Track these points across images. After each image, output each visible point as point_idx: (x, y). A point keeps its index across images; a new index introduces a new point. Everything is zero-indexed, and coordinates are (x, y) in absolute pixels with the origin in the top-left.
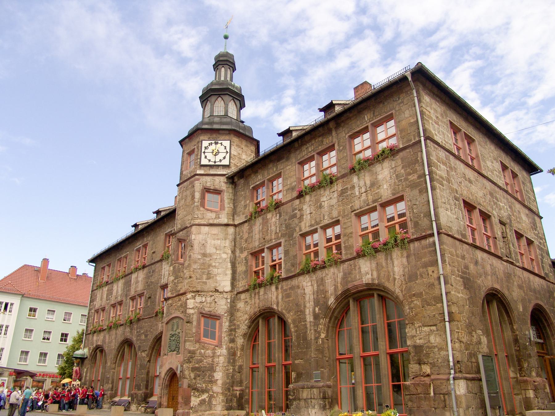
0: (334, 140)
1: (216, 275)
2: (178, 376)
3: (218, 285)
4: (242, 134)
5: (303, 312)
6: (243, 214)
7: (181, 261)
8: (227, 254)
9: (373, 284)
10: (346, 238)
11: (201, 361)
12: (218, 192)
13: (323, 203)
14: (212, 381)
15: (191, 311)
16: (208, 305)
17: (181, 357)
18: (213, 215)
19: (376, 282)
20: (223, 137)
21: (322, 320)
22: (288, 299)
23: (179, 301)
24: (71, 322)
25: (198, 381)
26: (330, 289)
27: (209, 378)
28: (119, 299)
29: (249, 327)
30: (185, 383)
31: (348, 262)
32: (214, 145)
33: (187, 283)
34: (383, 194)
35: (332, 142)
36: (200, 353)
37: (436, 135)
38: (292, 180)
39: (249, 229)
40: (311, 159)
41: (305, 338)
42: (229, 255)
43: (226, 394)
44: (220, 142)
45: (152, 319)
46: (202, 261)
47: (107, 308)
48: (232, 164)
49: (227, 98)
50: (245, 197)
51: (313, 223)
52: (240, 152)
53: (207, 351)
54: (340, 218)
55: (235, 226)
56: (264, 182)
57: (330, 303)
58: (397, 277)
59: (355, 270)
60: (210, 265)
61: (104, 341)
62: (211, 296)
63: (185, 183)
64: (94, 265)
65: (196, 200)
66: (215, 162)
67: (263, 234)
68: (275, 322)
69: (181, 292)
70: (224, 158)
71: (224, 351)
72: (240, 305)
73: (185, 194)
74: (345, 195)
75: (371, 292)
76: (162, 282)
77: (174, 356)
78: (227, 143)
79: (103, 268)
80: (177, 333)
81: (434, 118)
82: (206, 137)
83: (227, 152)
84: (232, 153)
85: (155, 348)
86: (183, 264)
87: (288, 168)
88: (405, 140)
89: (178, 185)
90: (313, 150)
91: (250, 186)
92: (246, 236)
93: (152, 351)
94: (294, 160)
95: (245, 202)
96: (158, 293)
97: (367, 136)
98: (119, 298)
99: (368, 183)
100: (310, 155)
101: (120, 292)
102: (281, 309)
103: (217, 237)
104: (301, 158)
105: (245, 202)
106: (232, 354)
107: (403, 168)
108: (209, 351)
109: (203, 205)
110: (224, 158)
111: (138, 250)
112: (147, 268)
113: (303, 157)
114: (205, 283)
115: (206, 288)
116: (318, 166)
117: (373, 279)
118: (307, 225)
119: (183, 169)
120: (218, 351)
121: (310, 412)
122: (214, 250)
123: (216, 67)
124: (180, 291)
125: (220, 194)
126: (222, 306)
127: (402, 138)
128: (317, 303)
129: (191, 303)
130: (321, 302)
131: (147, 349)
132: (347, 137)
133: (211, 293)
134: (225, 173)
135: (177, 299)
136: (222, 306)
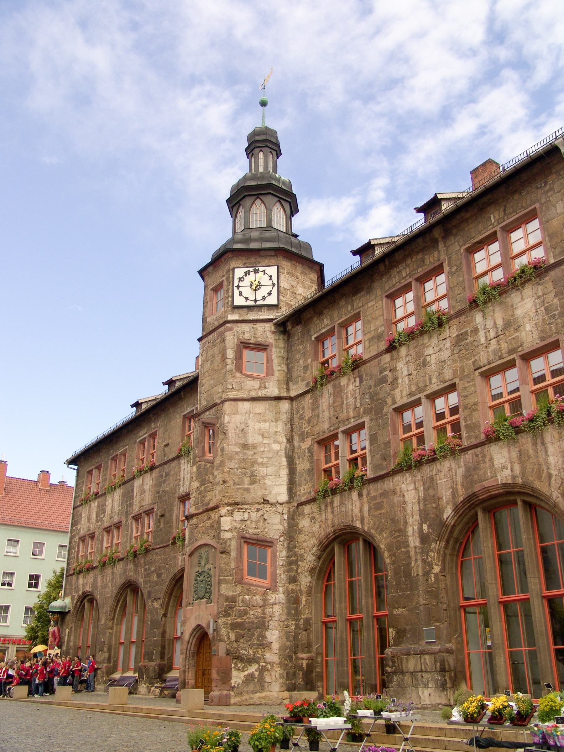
0: (442, 257)
1: (264, 478)
2: (211, 637)
3: (267, 492)
4: (295, 254)
5: (402, 532)
6: (303, 380)
7: (209, 456)
8: (280, 444)
9: (514, 485)
10: (467, 412)
11: (245, 613)
12: (261, 347)
13: (428, 358)
14: (264, 645)
15: (228, 535)
16: (254, 524)
17: (214, 607)
18: (256, 384)
19: (520, 481)
20: (266, 262)
21: (433, 545)
22: (379, 512)
23: (208, 519)
24: (43, 557)
25: (242, 645)
26: (446, 494)
27: (258, 640)
28: (116, 519)
29: (319, 558)
30: (221, 648)
31: (473, 451)
32: (252, 274)
33: (220, 492)
34: (524, 340)
35: (439, 260)
36: (244, 601)
38: (378, 323)
39: (313, 403)
40: (407, 288)
41: (408, 574)
42: (283, 446)
43: (287, 665)
44: (261, 269)
45: (167, 549)
46: (241, 456)
47: (97, 533)
48: (281, 303)
49: (269, 199)
50: (304, 354)
51: (414, 389)
52: (294, 283)
53: (254, 598)
54: (457, 381)
55: (291, 399)
56: (333, 328)
57: (445, 516)
58: (554, 472)
59: (484, 462)
60: (254, 463)
61: (94, 585)
62: (258, 510)
63: (211, 336)
64: (76, 467)
65: (229, 361)
66: (256, 301)
67: (335, 411)
68: (359, 548)
69: (211, 505)
70: (270, 294)
71: (281, 597)
72: (304, 523)
73: (210, 353)
74: (463, 343)
75: (512, 498)
76: (181, 491)
77: (203, 606)
78: (272, 271)
79: (90, 472)
80: (206, 569)
82: (240, 263)
83: (273, 285)
84: (282, 285)
85: (174, 594)
86: (212, 462)
87: (370, 304)
88: (558, 250)
89: (200, 340)
90: (410, 275)
91: (311, 336)
92: (308, 414)
93: (169, 599)
94: (379, 292)
95: (305, 361)
96: (175, 509)
97: (495, 247)
98: (116, 517)
99: (500, 322)
100: (404, 282)
101: (117, 509)
102: (369, 528)
103: (264, 418)
104: (390, 288)
105: (305, 361)
106: (293, 601)
107: (556, 296)
109: (239, 368)
110: (270, 294)
111: (143, 443)
112: (157, 469)
113: (393, 286)
114: (248, 490)
115: (249, 498)
116: (417, 300)
117: (514, 477)
118: (405, 393)
119: (207, 315)
120: (272, 597)
121: (420, 693)
122: (260, 439)
123: (250, 152)
124: (209, 503)
125: (265, 350)
126: (275, 525)
127: (554, 247)
128: (424, 516)
129: (226, 523)
130: (432, 516)
131: (162, 595)
132: (462, 251)
133: (257, 506)
134: (271, 317)
135: (205, 516)
136: (275, 525)
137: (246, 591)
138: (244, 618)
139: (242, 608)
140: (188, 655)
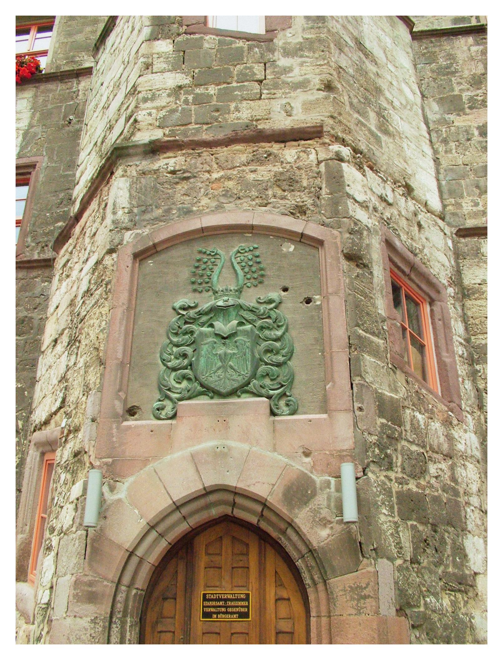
33: (308, 107)
36: (415, 428)
137: (415, 400)
138: (423, 482)
139: (414, 448)
140: (119, 606)
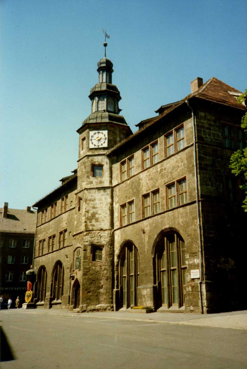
32: (97, 134)
37: (207, 138)
44: (101, 131)
66: (98, 146)
70: (104, 142)
80: (79, 257)
81: (207, 126)
83: (106, 138)
89: (78, 161)
108: (98, 268)
110: (104, 142)
